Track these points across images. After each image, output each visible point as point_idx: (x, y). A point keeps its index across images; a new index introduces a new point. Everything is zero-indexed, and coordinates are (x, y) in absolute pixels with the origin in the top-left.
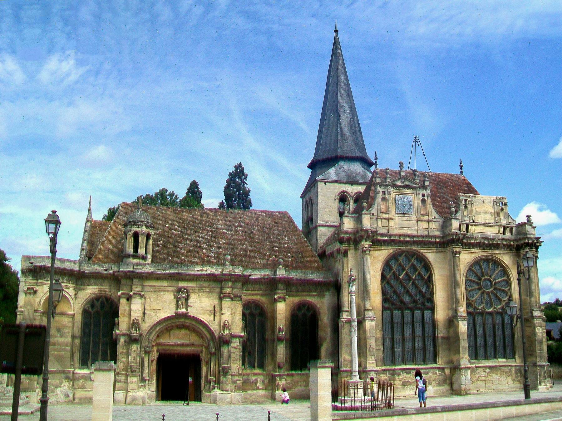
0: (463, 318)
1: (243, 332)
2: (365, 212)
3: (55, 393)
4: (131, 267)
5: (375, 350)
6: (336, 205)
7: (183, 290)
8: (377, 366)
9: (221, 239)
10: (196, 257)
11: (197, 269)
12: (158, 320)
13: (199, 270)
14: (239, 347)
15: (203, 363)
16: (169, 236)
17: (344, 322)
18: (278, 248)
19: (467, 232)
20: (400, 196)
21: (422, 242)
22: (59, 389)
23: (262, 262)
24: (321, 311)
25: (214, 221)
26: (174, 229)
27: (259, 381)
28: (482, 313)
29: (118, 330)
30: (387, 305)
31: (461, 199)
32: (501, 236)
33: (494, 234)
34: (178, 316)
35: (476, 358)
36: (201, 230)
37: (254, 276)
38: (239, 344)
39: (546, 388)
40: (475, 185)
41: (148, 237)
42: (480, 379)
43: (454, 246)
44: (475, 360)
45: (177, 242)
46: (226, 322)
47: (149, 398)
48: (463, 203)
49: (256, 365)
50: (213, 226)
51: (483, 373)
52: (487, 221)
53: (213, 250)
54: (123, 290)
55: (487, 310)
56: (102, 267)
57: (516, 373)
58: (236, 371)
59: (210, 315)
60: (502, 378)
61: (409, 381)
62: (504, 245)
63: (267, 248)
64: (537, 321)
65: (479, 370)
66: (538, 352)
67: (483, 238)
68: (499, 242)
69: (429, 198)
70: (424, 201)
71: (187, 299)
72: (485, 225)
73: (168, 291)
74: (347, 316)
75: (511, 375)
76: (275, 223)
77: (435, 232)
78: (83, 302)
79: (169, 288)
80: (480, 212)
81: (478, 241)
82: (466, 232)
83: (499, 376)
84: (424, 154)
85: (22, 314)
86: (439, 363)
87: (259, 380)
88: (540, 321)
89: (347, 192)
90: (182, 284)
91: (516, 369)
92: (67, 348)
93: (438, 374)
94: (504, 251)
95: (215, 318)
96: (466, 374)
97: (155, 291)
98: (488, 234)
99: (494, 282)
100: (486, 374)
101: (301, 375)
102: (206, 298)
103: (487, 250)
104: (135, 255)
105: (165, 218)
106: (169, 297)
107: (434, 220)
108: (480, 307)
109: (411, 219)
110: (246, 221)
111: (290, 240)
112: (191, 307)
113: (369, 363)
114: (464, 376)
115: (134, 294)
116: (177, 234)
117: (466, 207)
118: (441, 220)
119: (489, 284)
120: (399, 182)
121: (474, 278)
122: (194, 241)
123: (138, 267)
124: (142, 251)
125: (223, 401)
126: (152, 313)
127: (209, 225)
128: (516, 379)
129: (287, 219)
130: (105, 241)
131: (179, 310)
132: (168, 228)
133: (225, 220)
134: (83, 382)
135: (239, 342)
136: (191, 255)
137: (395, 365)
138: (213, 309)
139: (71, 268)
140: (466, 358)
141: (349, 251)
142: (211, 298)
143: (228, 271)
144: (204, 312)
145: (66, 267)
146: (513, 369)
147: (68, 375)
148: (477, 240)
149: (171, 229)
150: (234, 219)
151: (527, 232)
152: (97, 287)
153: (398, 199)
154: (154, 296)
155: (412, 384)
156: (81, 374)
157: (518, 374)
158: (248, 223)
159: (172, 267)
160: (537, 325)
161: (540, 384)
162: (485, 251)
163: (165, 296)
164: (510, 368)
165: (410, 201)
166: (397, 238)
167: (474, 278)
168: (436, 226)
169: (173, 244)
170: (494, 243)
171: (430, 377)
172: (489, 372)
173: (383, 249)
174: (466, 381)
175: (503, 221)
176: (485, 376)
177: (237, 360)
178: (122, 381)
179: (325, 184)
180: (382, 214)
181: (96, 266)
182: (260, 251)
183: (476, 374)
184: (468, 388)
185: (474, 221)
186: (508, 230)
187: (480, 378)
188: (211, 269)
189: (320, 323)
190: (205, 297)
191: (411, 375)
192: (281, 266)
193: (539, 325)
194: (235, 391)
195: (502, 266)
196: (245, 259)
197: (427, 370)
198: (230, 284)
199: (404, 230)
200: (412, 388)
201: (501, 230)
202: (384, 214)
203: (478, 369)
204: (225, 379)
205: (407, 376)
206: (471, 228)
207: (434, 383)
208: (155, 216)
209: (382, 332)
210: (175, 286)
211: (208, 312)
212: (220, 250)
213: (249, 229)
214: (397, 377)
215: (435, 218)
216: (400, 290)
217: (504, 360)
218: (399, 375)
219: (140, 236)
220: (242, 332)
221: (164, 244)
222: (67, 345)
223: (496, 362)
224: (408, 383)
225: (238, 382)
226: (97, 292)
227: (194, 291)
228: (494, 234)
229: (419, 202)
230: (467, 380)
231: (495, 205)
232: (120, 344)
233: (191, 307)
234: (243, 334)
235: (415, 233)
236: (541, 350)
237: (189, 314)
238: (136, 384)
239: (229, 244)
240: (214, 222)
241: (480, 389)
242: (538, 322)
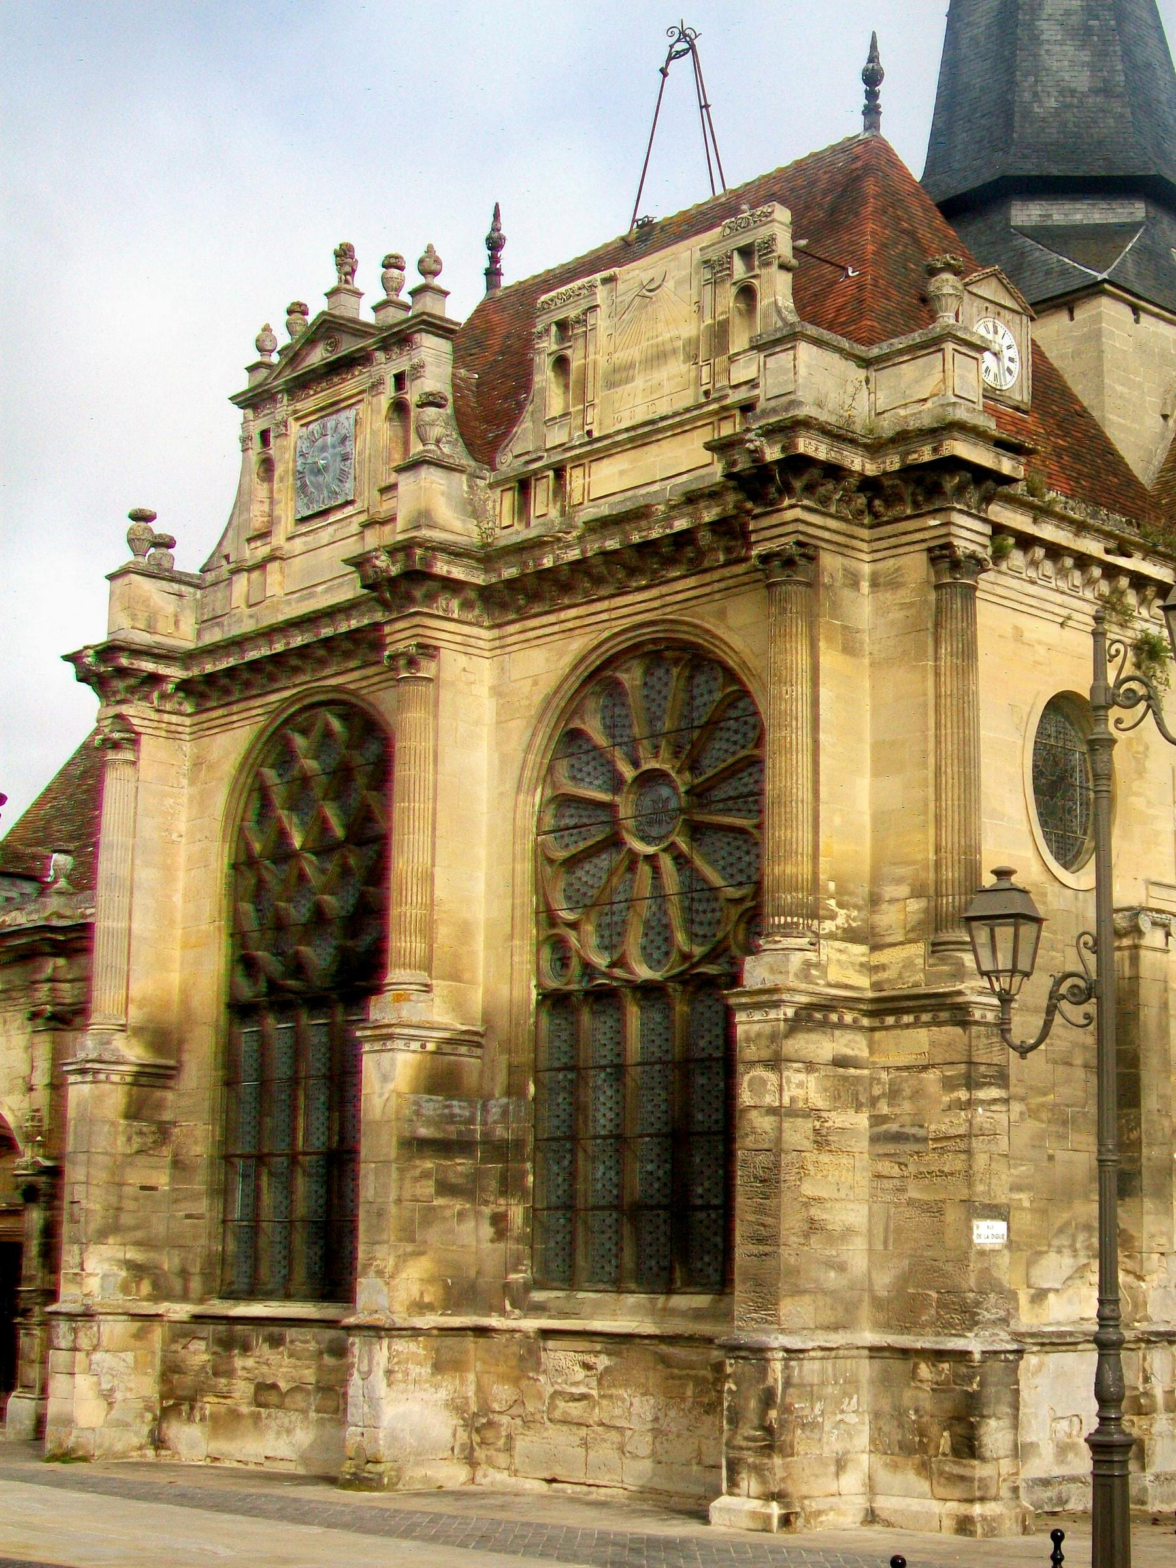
33: (684, 478)
35: (570, 1282)
39: (754, 1515)
42: (557, 1414)
51: (580, 1374)
64: (756, 1027)
65: (559, 1356)
68: (681, 524)
80: (631, 366)
81: (574, 554)
103: (640, 589)
117: (561, 364)
148: (569, 546)
161: (733, 1483)
170: (655, 534)
172: (607, 1369)
173: (235, 718)
183: (542, 1378)
187: (561, 1404)
200: (286, 1420)
203: (551, 1344)
214: (239, 1362)
218: (246, 1348)
224: (273, 1398)
236: (761, 1240)
241: (559, 1472)
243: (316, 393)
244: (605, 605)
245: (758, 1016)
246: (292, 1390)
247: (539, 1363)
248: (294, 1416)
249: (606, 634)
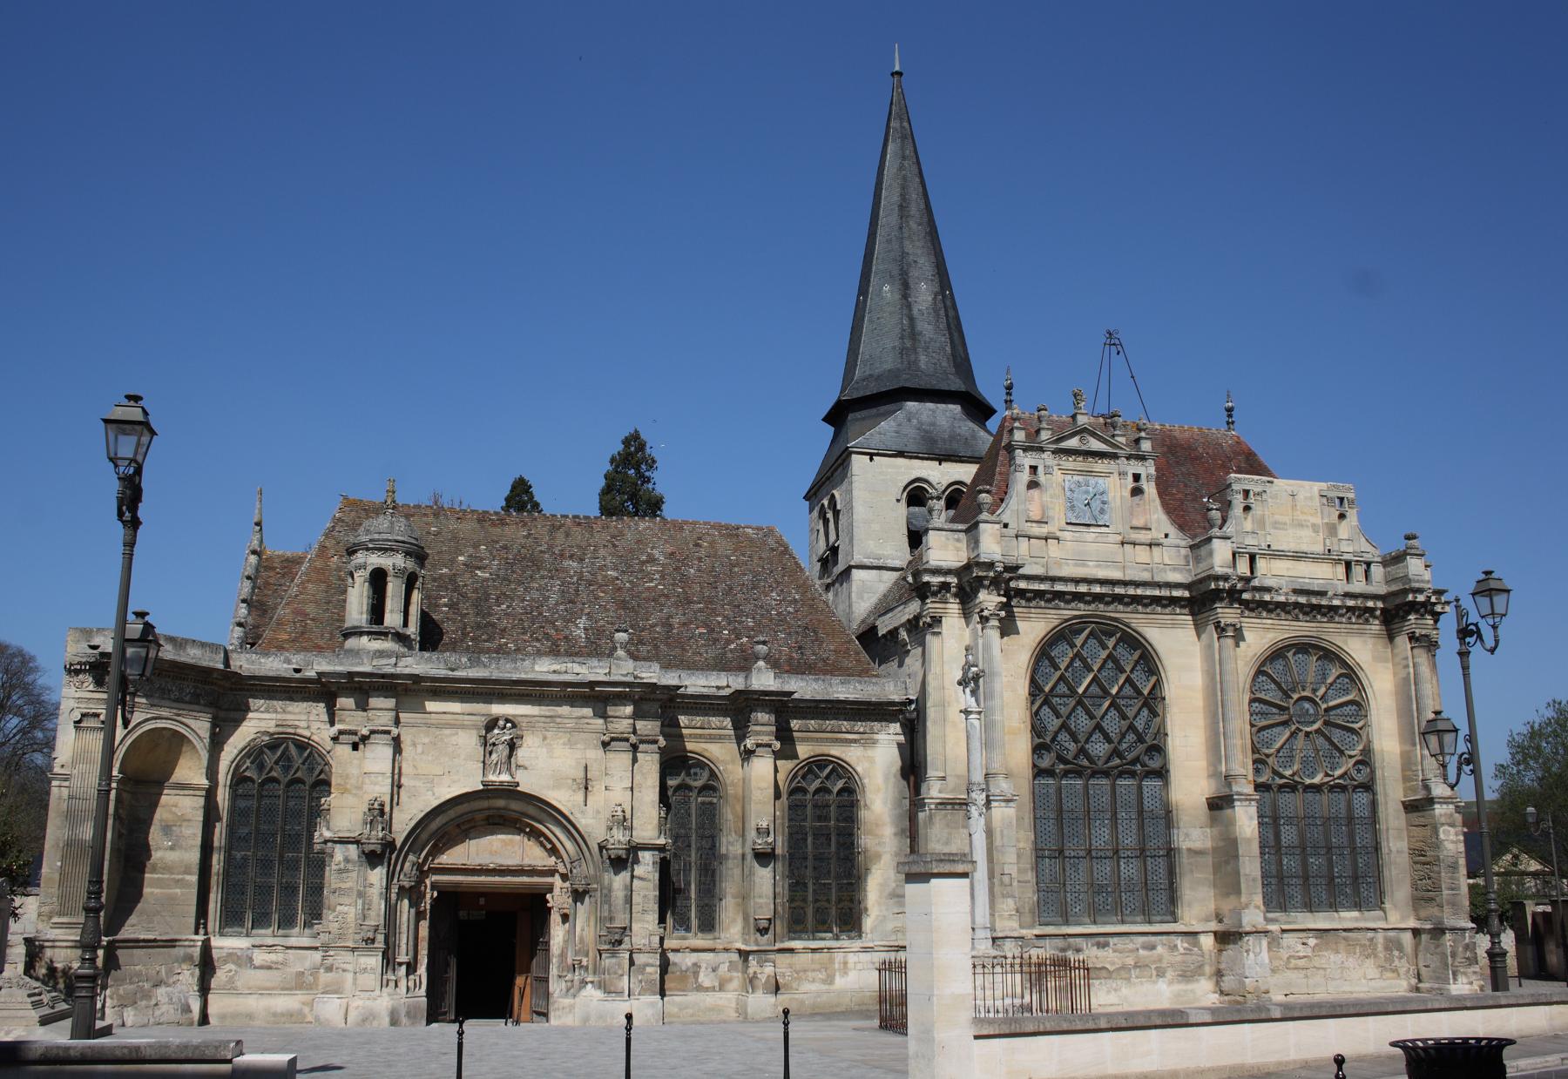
0: (1247, 800)
1: (662, 835)
2: (984, 516)
3: (153, 1002)
4: (365, 661)
5: (1015, 883)
6: (900, 513)
7: (501, 723)
8: (1021, 927)
9: (602, 595)
10: (537, 640)
11: (544, 669)
12: (435, 803)
13: (545, 669)
14: (651, 877)
15: (555, 918)
16: (466, 585)
17: (933, 807)
18: (753, 618)
19: (1252, 572)
20: (1076, 478)
21: (1136, 600)
22: (161, 992)
23: (710, 653)
24: (866, 781)
25: (585, 549)
26: (479, 568)
27: (703, 969)
28: (1292, 787)
29: (328, 829)
30: (1045, 763)
31: (1235, 487)
32: (1343, 587)
33: (1321, 581)
34: (489, 792)
35: (1283, 908)
36: (550, 571)
37: (690, 691)
38: (650, 868)
40: (1264, 458)
41: (411, 582)
42: (1291, 965)
43: (1219, 610)
44: (1278, 914)
45: (487, 600)
46: (619, 809)
47: (408, 1014)
48: (1240, 497)
49: (694, 922)
50: (582, 560)
51: (1300, 947)
52: (1304, 548)
53: (582, 622)
54: (342, 721)
55: (1308, 781)
56: (288, 661)
57: (1387, 948)
58: (643, 941)
59: (574, 791)
60: (1351, 962)
61: (1104, 968)
62: (1349, 609)
63: (725, 617)
64: (1443, 812)
65: (1289, 939)
66: (1445, 892)
67: (1296, 592)
68: (1336, 602)
69: (1153, 484)
70: (1137, 491)
71: (512, 746)
72: (1298, 556)
73: (463, 727)
74: (940, 792)
75: (1376, 956)
76: (744, 555)
77: (1168, 572)
78: (233, 756)
79: (466, 717)
80: (1285, 524)
81: (1282, 599)
82: (1249, 574)
83: (1341, 957)
84: (1133, 377)
85: (67, 784)
86: (1182, 919)
87: (704, 966)
88: (1449, 812)
89: (926, 481)
90: (498, 709)
91: (1388, 940)
92: (188, 877)
93: (1182, 950)
94: (1348, 626)
95: (589, 798)
96: (1258, 950)
97: (429, 726)
98: (1307, 581)
99: (1324, 706)
100: (1309, 950)
101: (814, 950)
102: (564, 744)
103: (1307, 621)
104: (375, 628)
105: (455, 538)
106: (467, 742)
107: (1165, 541)
108: (1288, 773)
109: (1105, 540)
110: (669, 549)
111: (783, 600)
112: (526, 768)
113: (1000, 916)
114: (1251, 954)
115: (373, 732)
116: (487, 580)
118: (1183, 543)
119: (1311, 711)
120: (1073, 443)
121: (1272, 695)
122: (533, 600)
123: (384, 661)
124: (392, 619)
125: (609, 1020)
126: (419, 784)
127: (571, 557)
128: (1387, 966)
129: (775, 546)
130: (297, 596)
131: (492, 777)
132: (464, 565)
133: (614, 546)
134: (231, 971)
135: (651, 863)
136: (523, 633)
137: (1067, 923)
138: (582, 774)
139: (205, 664)
140: (1257, 907)
141: (944, 619)
142: (579, 746)
143: (622, 675)
144: (558, 782)
145: (192, 661)
146: (1380, 936)
147: (190, 950)
148: (1279, 595)
149: (470, 567)
150: (638, 542)
151: (1411, 576)
152: (274, 716)
153: (1072, 486)
154: (426, 740)
155: (1114, 975)
156: (226, 951)
157: (1392, 951)
158: (672, 554)
159: (475, 662)
160: (1443, 820)
161: (1455, 979)
162: (1300, 624)
163: (455, 738)
164: (1370, 934)
165: (1102, 494)
166: (1071, 588)
167: (1272, 695)
168: (1170, 559)
169: (476, 605)
171: (1160, 959)
172: (1316, 945)
174: (1258, 969)
175: (1345, 547)
176: (1305, 957)
177: (644, 911)
178: (337, 968)
179: (871, 459)
180: (1029, 524)
181: (270, 659)
182: (706, 626)
184: (1263, 988)
185: (1269, 546)
186: (1358, 571)
187: (1293, 961)
188: (577, 668)
189: (863, 814)
190: (561, 741)
191: (1111, 951)
192: (761, 663)
193: (1448, 821)
194: (639, 994)
195: (1344, 664)
196: (667, 644)
197: (1153, 939)
198: (629, 710)
199: (1088, 566)
200: (1114, 985)
201: (1341, 569)
202: (1034, 525)
203: (1285, 935)
204: (614, 960)
205: (1101, 953)
206: (1261, 564)
207: (1170, 974)
208: (428, 533)
209: (1033, 837)
210: (484, 712)
211: (570, 781)
212: (602, 623)
213: (677, 569)
215: (1166, 536)
216: (1082, 723)
217: (1355, 914)
219: (389, 579)
220: (659, 837)
221: (452, 606)
222: (187, 871)
223: (1333, 919)
224: (1104, 973)
225: (649, 969)
226: (271, 730)
227: (532, 727)
228: (1321, 581)
229: (1127, 493)
230: (1261, 966)
231: (1324, 505)
232: (334, 867)
233: (526, 768)
234: (662, 841)
235: (1116, 575)
236: (1453, 889)
237: (519, 788)
238: (373, 976)
239: (623, 605)
240: (583, 549)
242: (1445, 814)
243: (1075, 460)
244: (1287, 623)
245: (1445, 806)
246: (1118, 969)
247: (1279, 944)
248: (1119, 982)
249: (1286, 636)
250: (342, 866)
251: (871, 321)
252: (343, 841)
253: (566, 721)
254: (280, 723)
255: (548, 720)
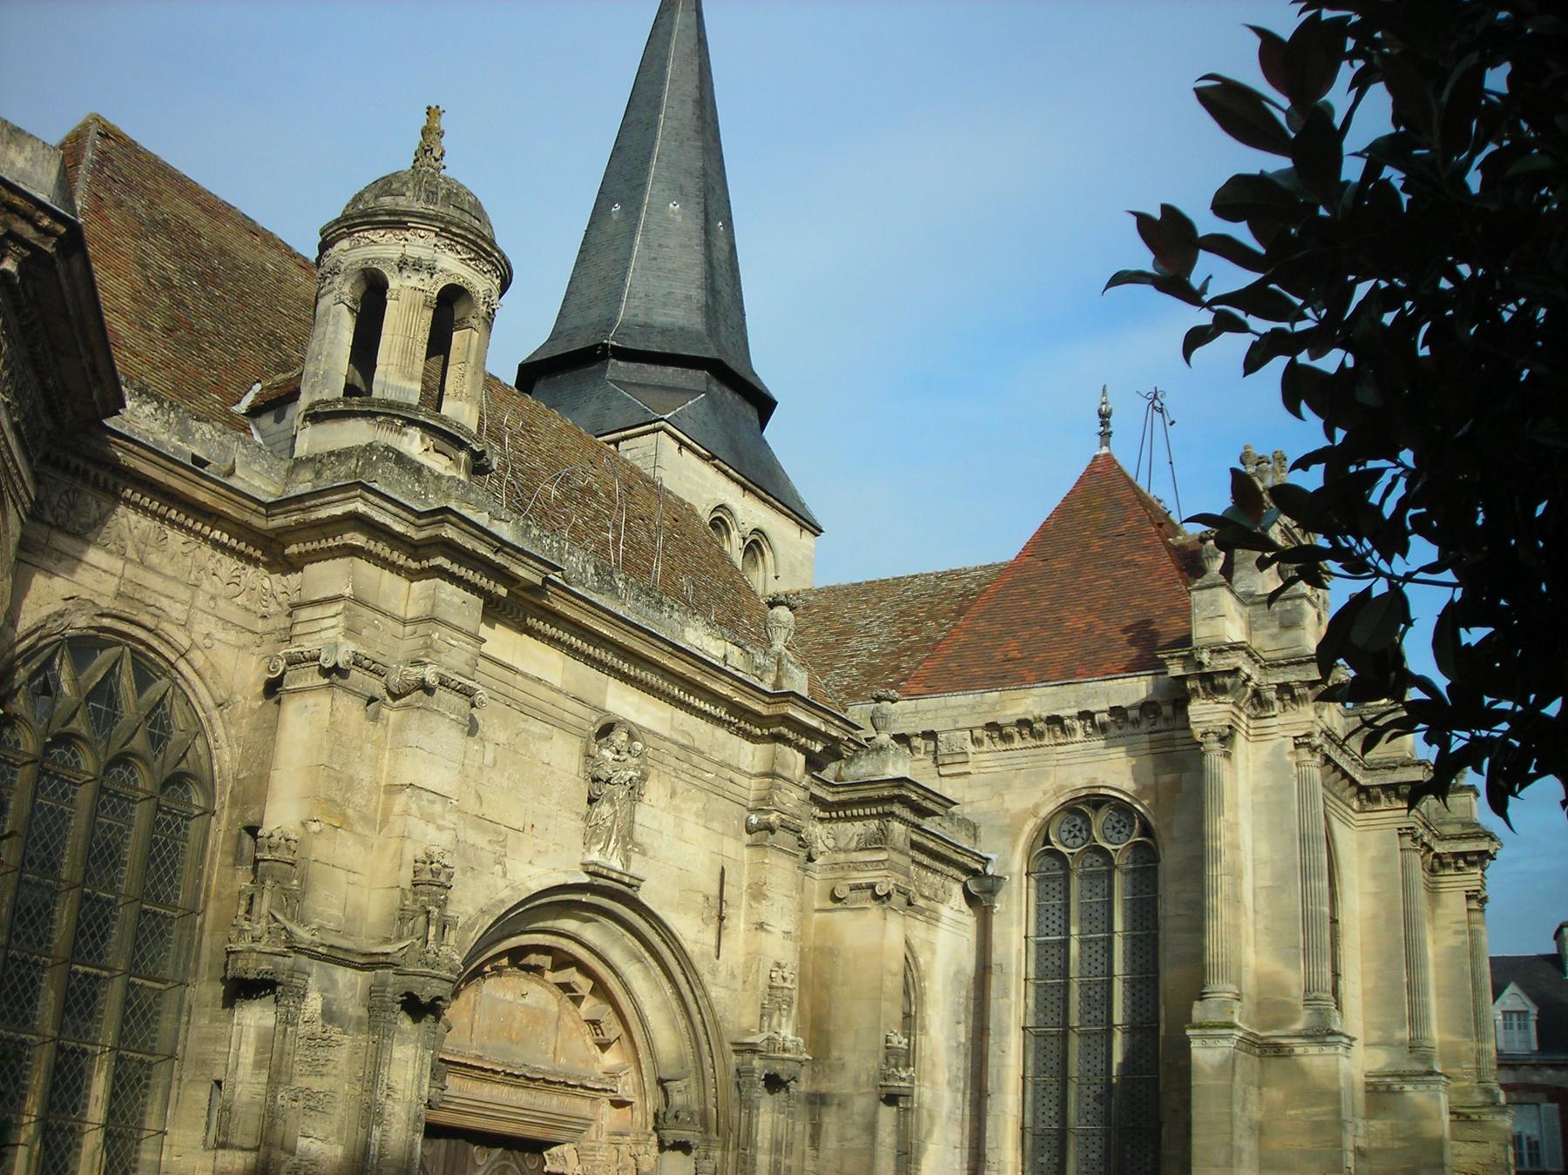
56: (186, 434)
73: (562, 726)
90: (624, 702)
152: (117, 564)
211: (701, 899)
250: (317, 1028)
251: (646, 245)
252: (336, 957)
253: (705, 765)
254: (128, 589)
255: (682, 754)
